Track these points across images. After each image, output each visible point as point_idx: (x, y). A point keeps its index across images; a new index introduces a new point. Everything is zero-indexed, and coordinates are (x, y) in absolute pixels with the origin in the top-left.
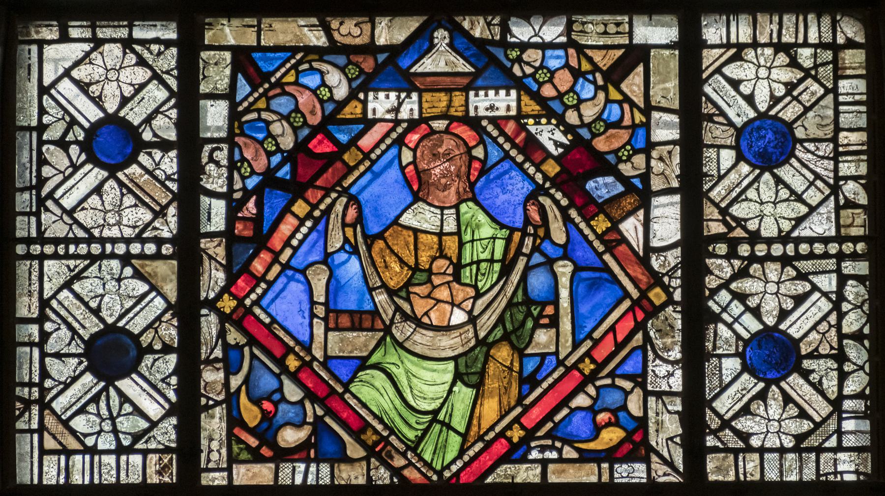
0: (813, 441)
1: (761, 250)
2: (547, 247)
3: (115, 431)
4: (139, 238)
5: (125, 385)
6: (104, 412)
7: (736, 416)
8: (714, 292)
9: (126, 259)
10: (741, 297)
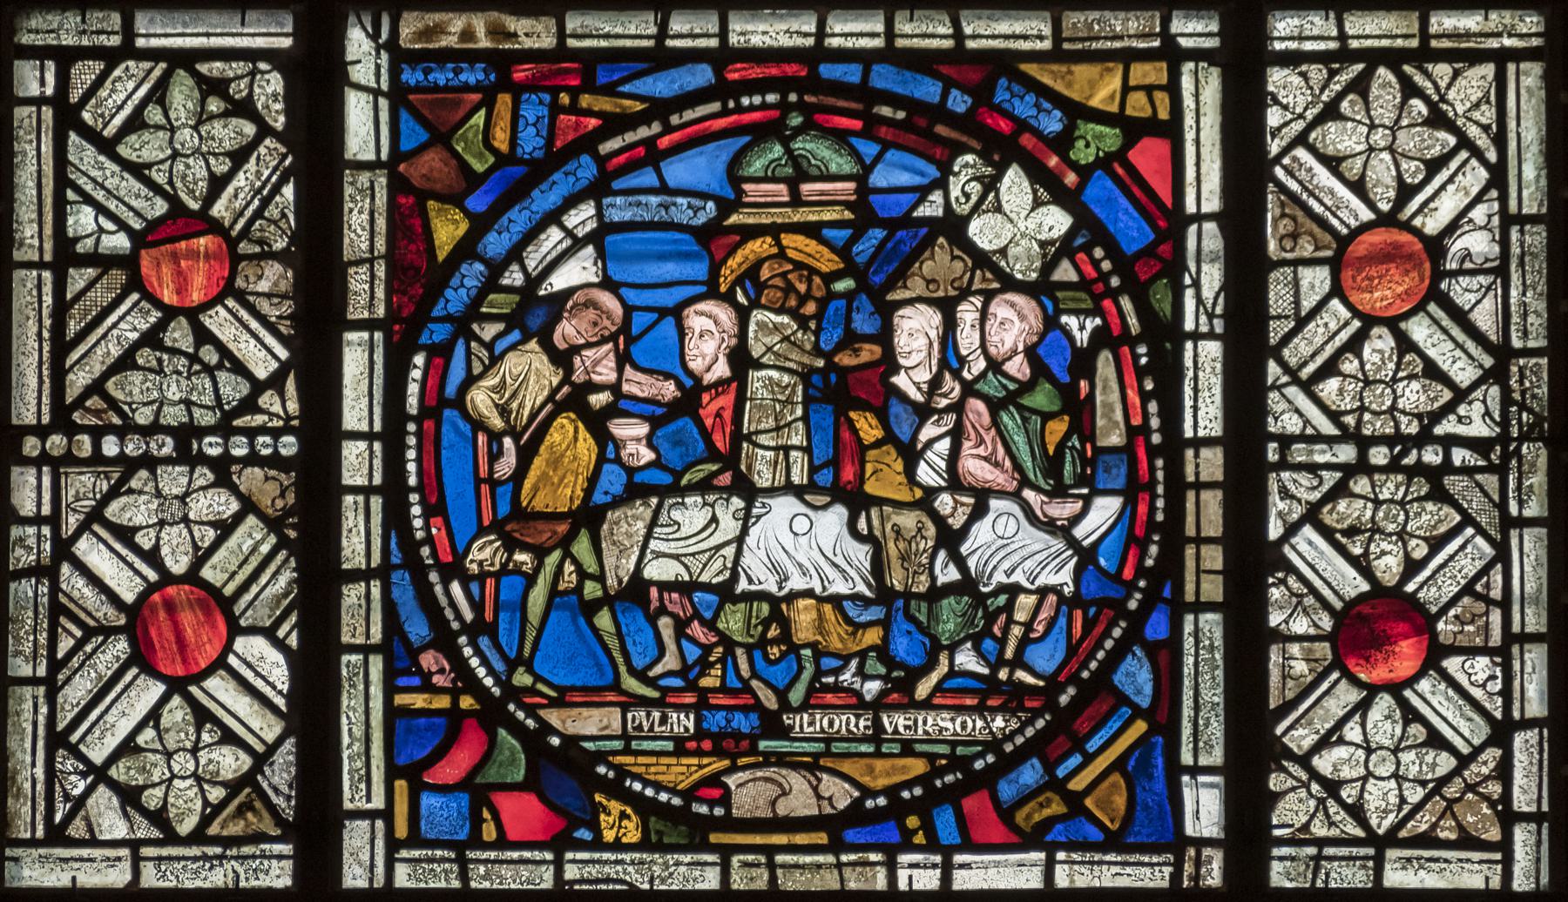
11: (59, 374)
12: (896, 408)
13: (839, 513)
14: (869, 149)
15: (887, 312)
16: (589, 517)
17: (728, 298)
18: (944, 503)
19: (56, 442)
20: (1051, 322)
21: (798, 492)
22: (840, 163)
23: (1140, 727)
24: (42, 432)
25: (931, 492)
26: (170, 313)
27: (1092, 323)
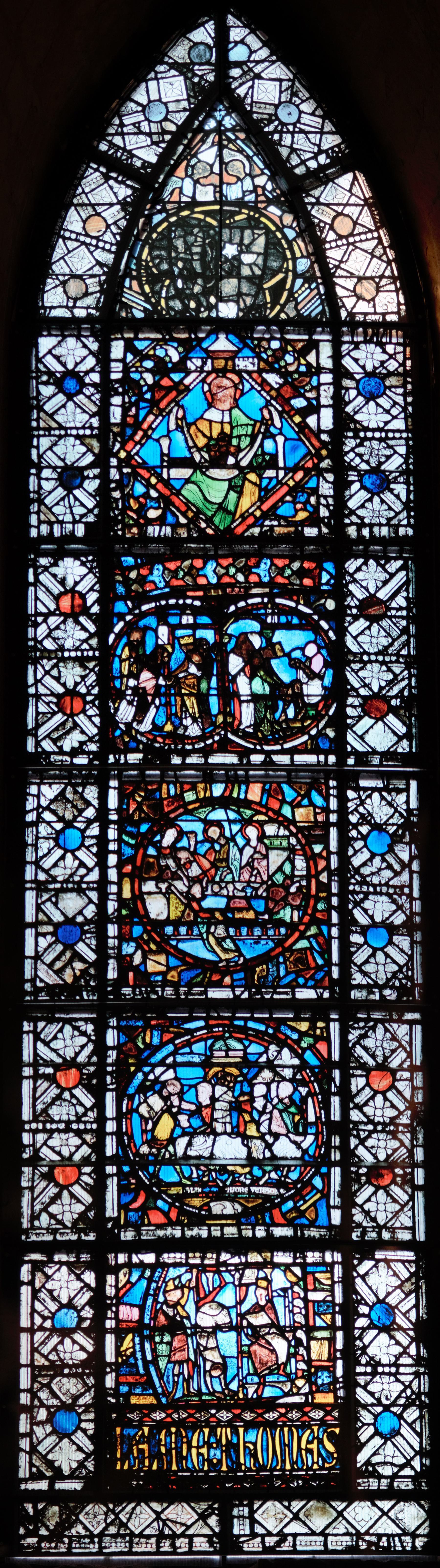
0: (395, 521)
1: (370, 435)
2: (272, 430)
3: (72, 513)
4: (84, 428)
5: (77, 492)
6: (67, 505)
7: (358, 508)
8: (348, 452)
9: (77, 437)
10: (361, 456)
11: (34, 1106)
12: (255, 1113)
13: (239, 1140)
14: (247, 1043)
15: (252, 1086)
16: (172, 1140)
17: (209, 1082)
18: (267, 1137)
19: (34, 1126)
20: (295, 1089)
21: (229, 1135)
22: (239, 1046)
23: (319, 1195)
24: (30, 1122)
25: (264, 1135)
26: (63, 1090)
27: (306, 1089)
